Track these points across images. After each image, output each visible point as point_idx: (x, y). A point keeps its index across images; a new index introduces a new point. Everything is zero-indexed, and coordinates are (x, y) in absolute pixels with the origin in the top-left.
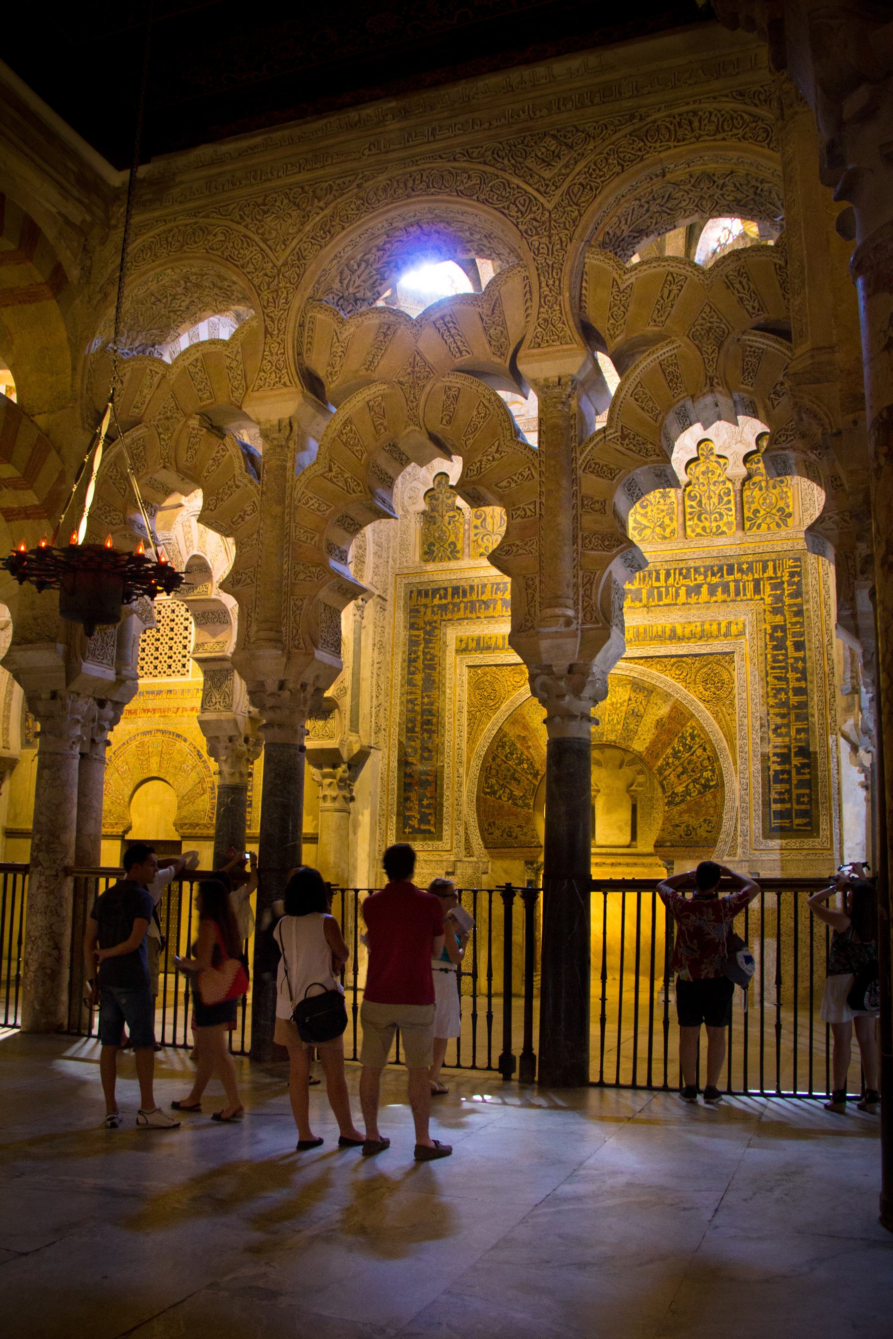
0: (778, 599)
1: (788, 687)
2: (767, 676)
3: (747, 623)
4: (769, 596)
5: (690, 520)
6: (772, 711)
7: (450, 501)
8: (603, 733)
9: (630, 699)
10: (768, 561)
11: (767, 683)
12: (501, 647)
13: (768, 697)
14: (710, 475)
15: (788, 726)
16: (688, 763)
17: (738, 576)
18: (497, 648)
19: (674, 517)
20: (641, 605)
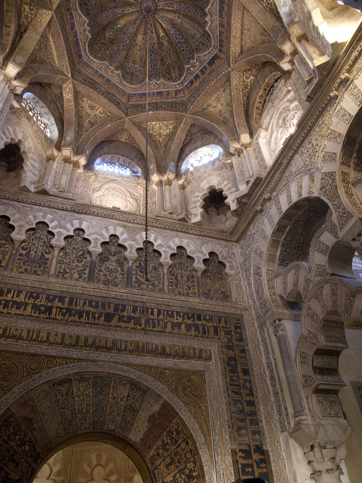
0: (230, 340)
1: (242, 399)
2: (228, 390)
3: (212, 351)
4: (224, 337)
5: (170, 286)
6: (233, 415)
7: (5, 235)
8: (104, 423)
9: (128, 396)
10: (221, 317)
11: (228, 394)
12: (25, 337)
13: (230, 405)
14: (182, 265)
15: (246, 428)
16: (175, 455)
17: (204, 322)
18: (20, 338)
19: (161, 282)
20: (140, 327)
